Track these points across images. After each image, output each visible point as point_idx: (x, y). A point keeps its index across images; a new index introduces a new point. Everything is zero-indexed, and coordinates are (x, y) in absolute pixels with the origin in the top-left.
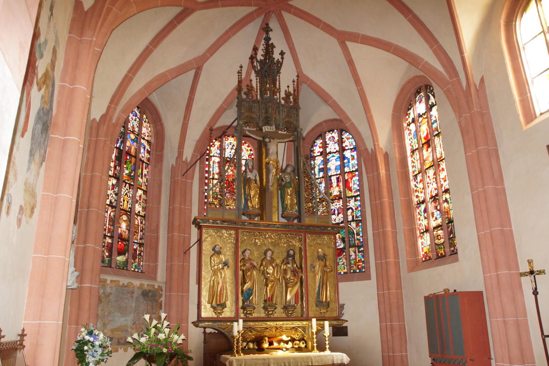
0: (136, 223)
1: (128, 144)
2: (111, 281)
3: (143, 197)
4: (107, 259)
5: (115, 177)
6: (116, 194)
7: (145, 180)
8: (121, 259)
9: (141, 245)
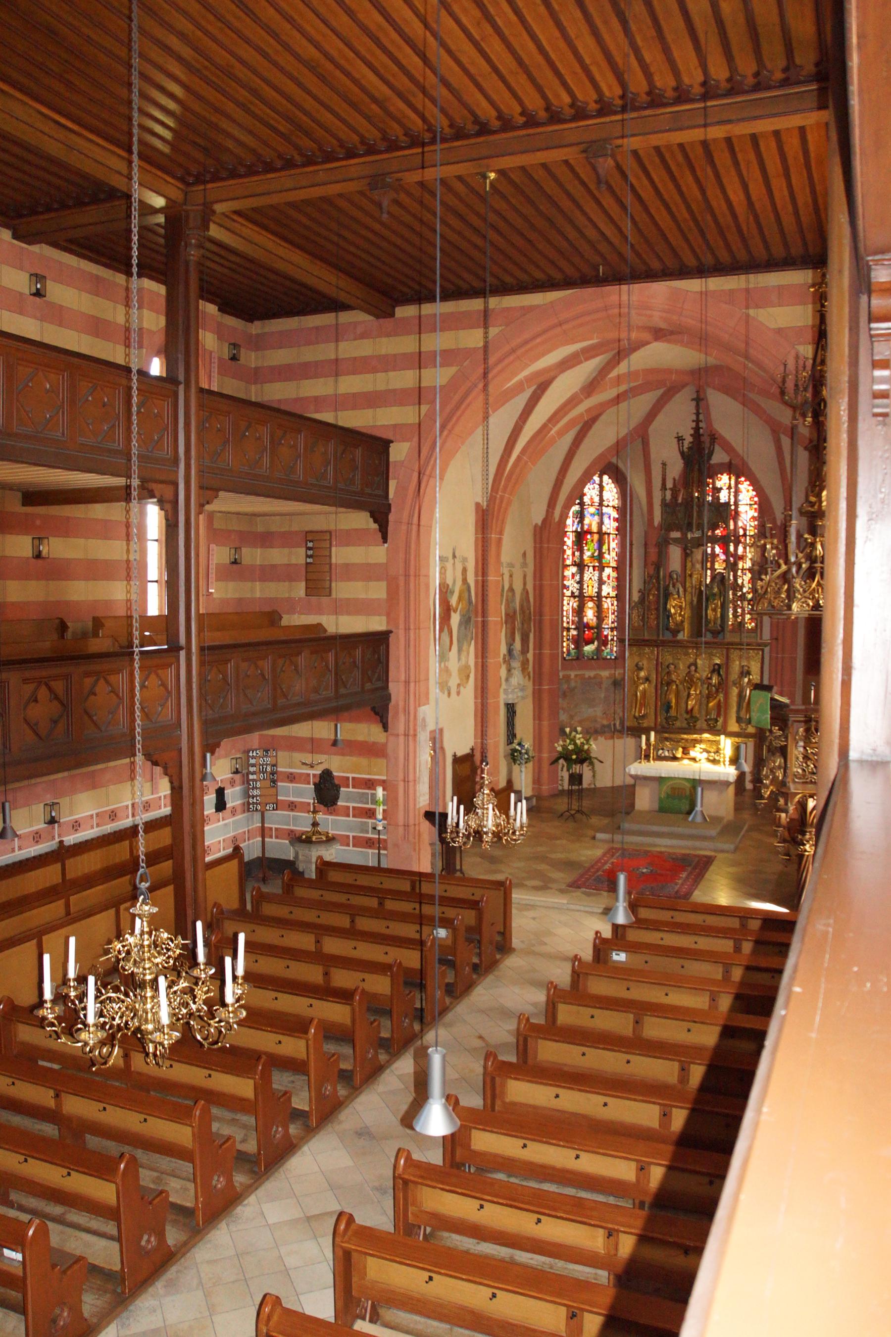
0: (605, 606)
1: (587, 521)
2: (576, 676)
3: (614, 575)
4: (573, 652)
5: (575, 564)
6: (578, 583)
7: (613, 554)
8: (589, 648)
9: (612, 629)
